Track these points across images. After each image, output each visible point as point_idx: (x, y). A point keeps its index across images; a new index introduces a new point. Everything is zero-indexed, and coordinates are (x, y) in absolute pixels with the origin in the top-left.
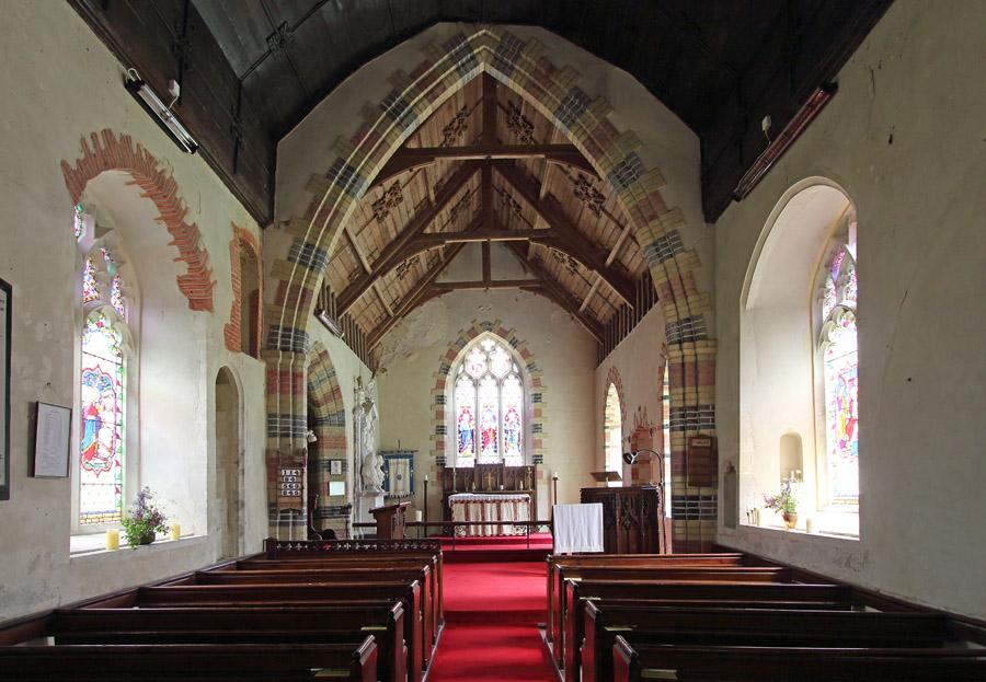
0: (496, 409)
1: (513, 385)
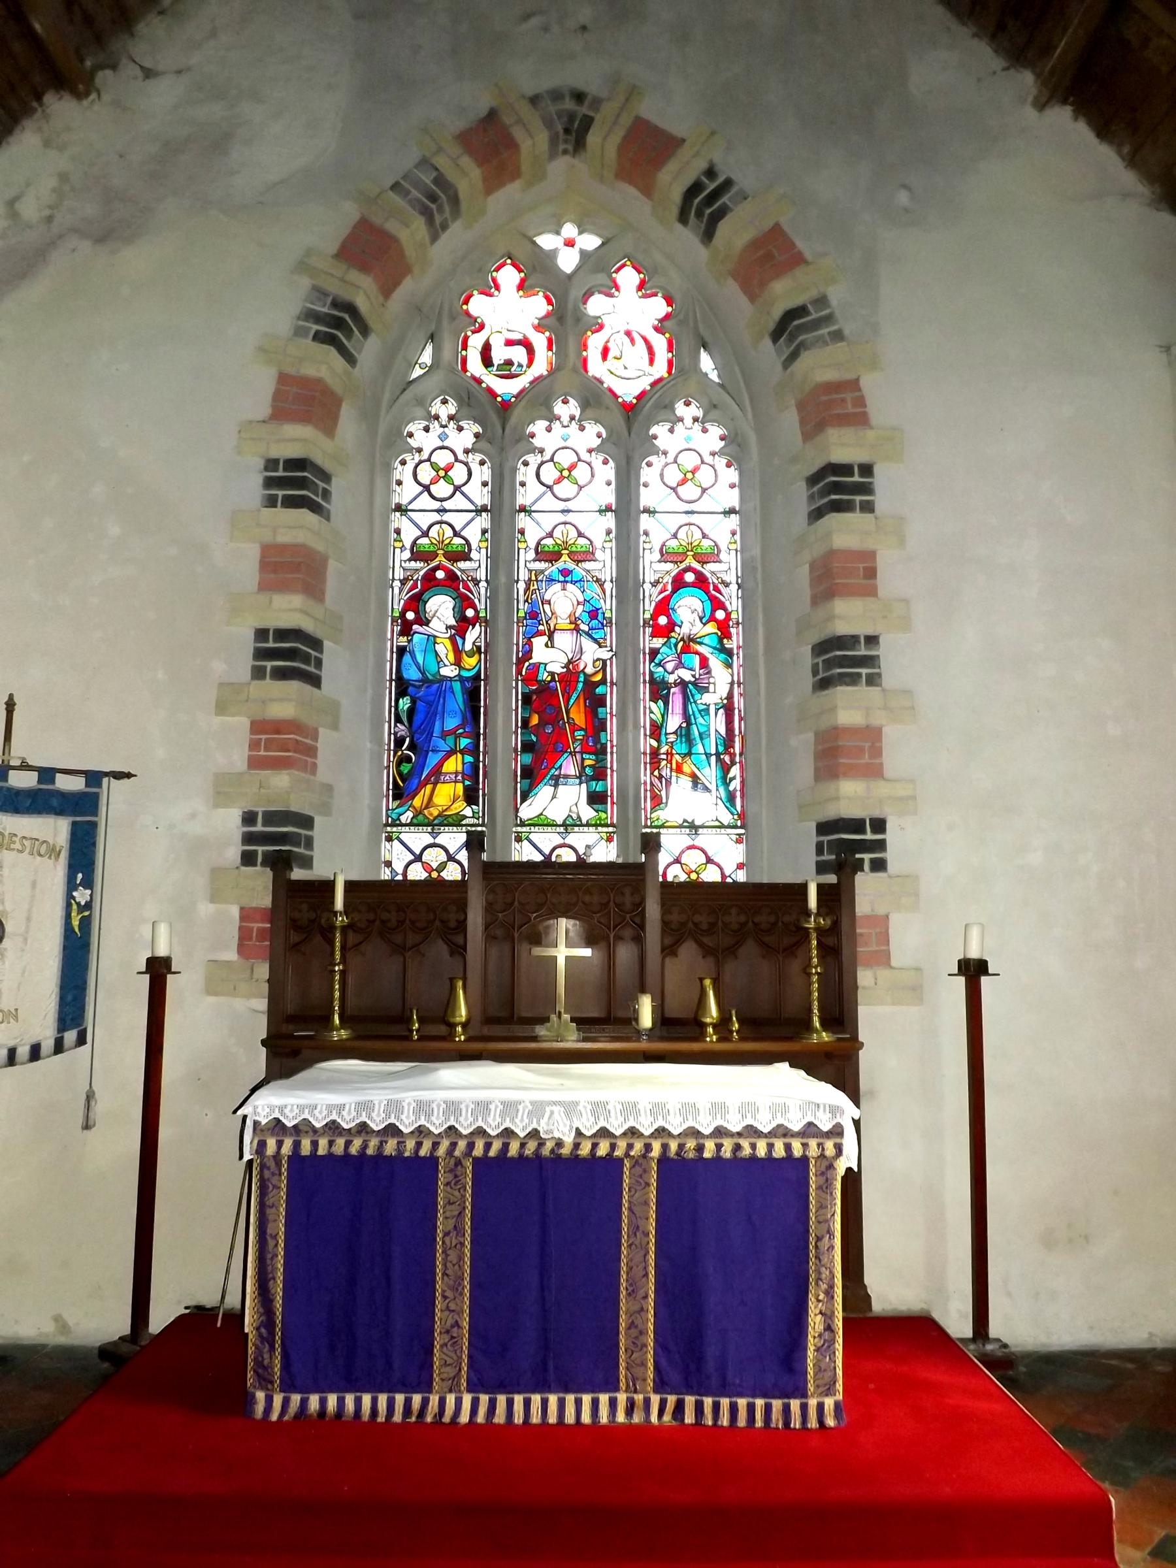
0: (605, 565)
1: (689, 441)
